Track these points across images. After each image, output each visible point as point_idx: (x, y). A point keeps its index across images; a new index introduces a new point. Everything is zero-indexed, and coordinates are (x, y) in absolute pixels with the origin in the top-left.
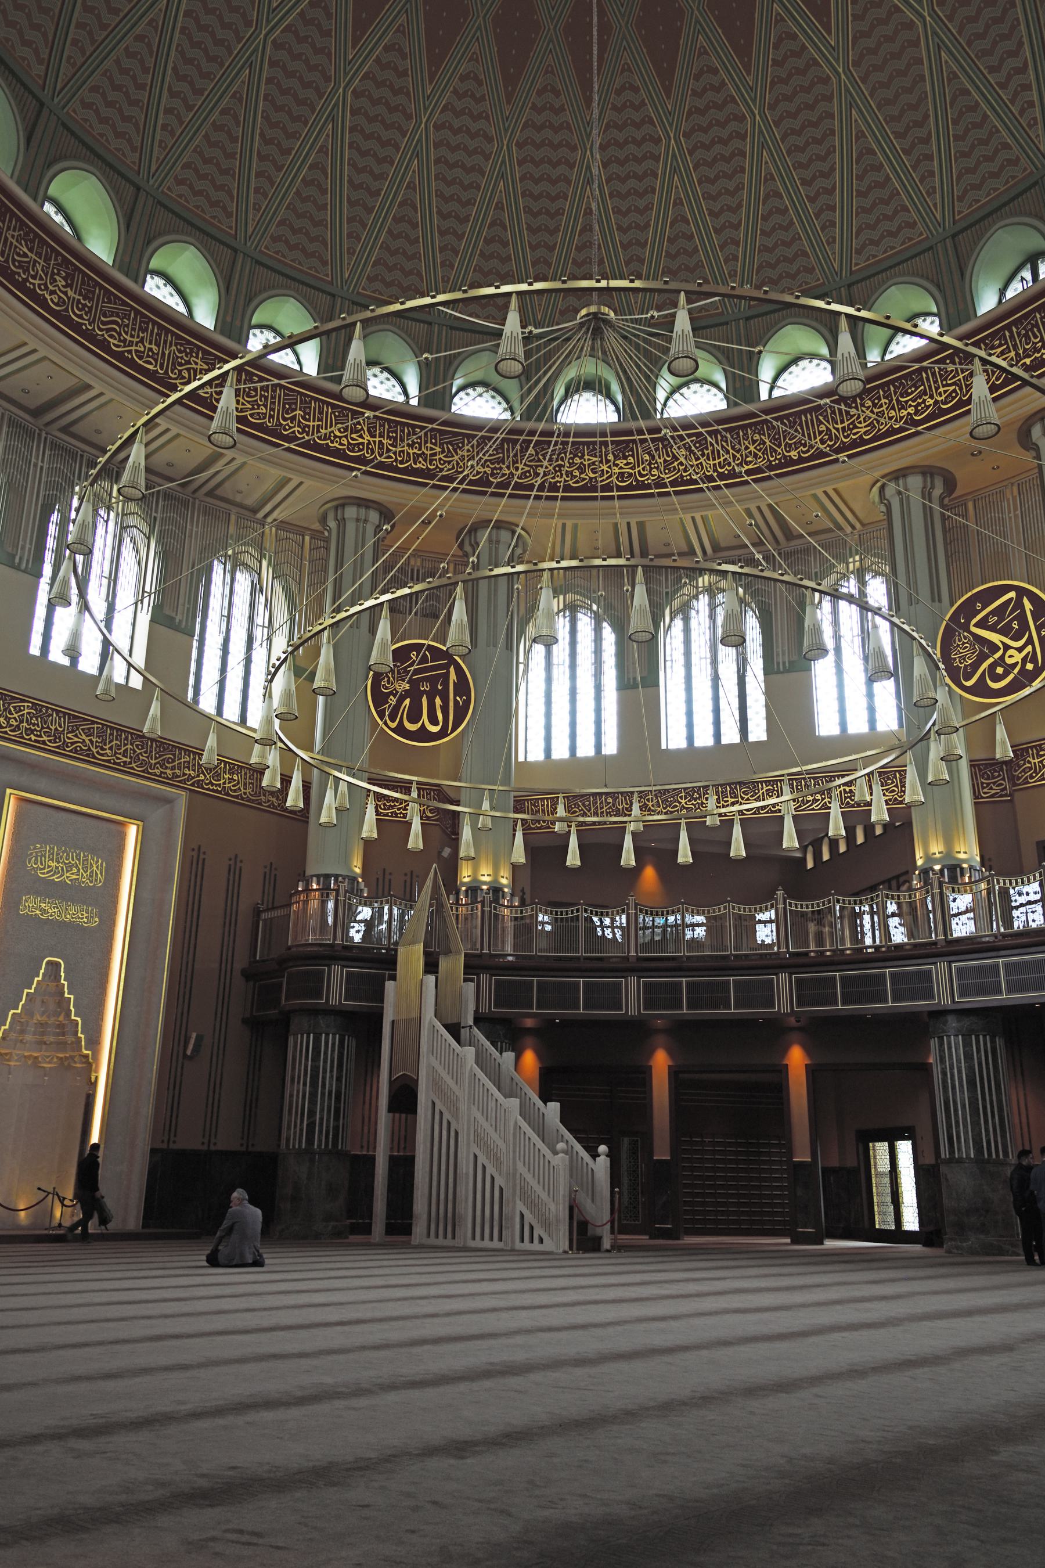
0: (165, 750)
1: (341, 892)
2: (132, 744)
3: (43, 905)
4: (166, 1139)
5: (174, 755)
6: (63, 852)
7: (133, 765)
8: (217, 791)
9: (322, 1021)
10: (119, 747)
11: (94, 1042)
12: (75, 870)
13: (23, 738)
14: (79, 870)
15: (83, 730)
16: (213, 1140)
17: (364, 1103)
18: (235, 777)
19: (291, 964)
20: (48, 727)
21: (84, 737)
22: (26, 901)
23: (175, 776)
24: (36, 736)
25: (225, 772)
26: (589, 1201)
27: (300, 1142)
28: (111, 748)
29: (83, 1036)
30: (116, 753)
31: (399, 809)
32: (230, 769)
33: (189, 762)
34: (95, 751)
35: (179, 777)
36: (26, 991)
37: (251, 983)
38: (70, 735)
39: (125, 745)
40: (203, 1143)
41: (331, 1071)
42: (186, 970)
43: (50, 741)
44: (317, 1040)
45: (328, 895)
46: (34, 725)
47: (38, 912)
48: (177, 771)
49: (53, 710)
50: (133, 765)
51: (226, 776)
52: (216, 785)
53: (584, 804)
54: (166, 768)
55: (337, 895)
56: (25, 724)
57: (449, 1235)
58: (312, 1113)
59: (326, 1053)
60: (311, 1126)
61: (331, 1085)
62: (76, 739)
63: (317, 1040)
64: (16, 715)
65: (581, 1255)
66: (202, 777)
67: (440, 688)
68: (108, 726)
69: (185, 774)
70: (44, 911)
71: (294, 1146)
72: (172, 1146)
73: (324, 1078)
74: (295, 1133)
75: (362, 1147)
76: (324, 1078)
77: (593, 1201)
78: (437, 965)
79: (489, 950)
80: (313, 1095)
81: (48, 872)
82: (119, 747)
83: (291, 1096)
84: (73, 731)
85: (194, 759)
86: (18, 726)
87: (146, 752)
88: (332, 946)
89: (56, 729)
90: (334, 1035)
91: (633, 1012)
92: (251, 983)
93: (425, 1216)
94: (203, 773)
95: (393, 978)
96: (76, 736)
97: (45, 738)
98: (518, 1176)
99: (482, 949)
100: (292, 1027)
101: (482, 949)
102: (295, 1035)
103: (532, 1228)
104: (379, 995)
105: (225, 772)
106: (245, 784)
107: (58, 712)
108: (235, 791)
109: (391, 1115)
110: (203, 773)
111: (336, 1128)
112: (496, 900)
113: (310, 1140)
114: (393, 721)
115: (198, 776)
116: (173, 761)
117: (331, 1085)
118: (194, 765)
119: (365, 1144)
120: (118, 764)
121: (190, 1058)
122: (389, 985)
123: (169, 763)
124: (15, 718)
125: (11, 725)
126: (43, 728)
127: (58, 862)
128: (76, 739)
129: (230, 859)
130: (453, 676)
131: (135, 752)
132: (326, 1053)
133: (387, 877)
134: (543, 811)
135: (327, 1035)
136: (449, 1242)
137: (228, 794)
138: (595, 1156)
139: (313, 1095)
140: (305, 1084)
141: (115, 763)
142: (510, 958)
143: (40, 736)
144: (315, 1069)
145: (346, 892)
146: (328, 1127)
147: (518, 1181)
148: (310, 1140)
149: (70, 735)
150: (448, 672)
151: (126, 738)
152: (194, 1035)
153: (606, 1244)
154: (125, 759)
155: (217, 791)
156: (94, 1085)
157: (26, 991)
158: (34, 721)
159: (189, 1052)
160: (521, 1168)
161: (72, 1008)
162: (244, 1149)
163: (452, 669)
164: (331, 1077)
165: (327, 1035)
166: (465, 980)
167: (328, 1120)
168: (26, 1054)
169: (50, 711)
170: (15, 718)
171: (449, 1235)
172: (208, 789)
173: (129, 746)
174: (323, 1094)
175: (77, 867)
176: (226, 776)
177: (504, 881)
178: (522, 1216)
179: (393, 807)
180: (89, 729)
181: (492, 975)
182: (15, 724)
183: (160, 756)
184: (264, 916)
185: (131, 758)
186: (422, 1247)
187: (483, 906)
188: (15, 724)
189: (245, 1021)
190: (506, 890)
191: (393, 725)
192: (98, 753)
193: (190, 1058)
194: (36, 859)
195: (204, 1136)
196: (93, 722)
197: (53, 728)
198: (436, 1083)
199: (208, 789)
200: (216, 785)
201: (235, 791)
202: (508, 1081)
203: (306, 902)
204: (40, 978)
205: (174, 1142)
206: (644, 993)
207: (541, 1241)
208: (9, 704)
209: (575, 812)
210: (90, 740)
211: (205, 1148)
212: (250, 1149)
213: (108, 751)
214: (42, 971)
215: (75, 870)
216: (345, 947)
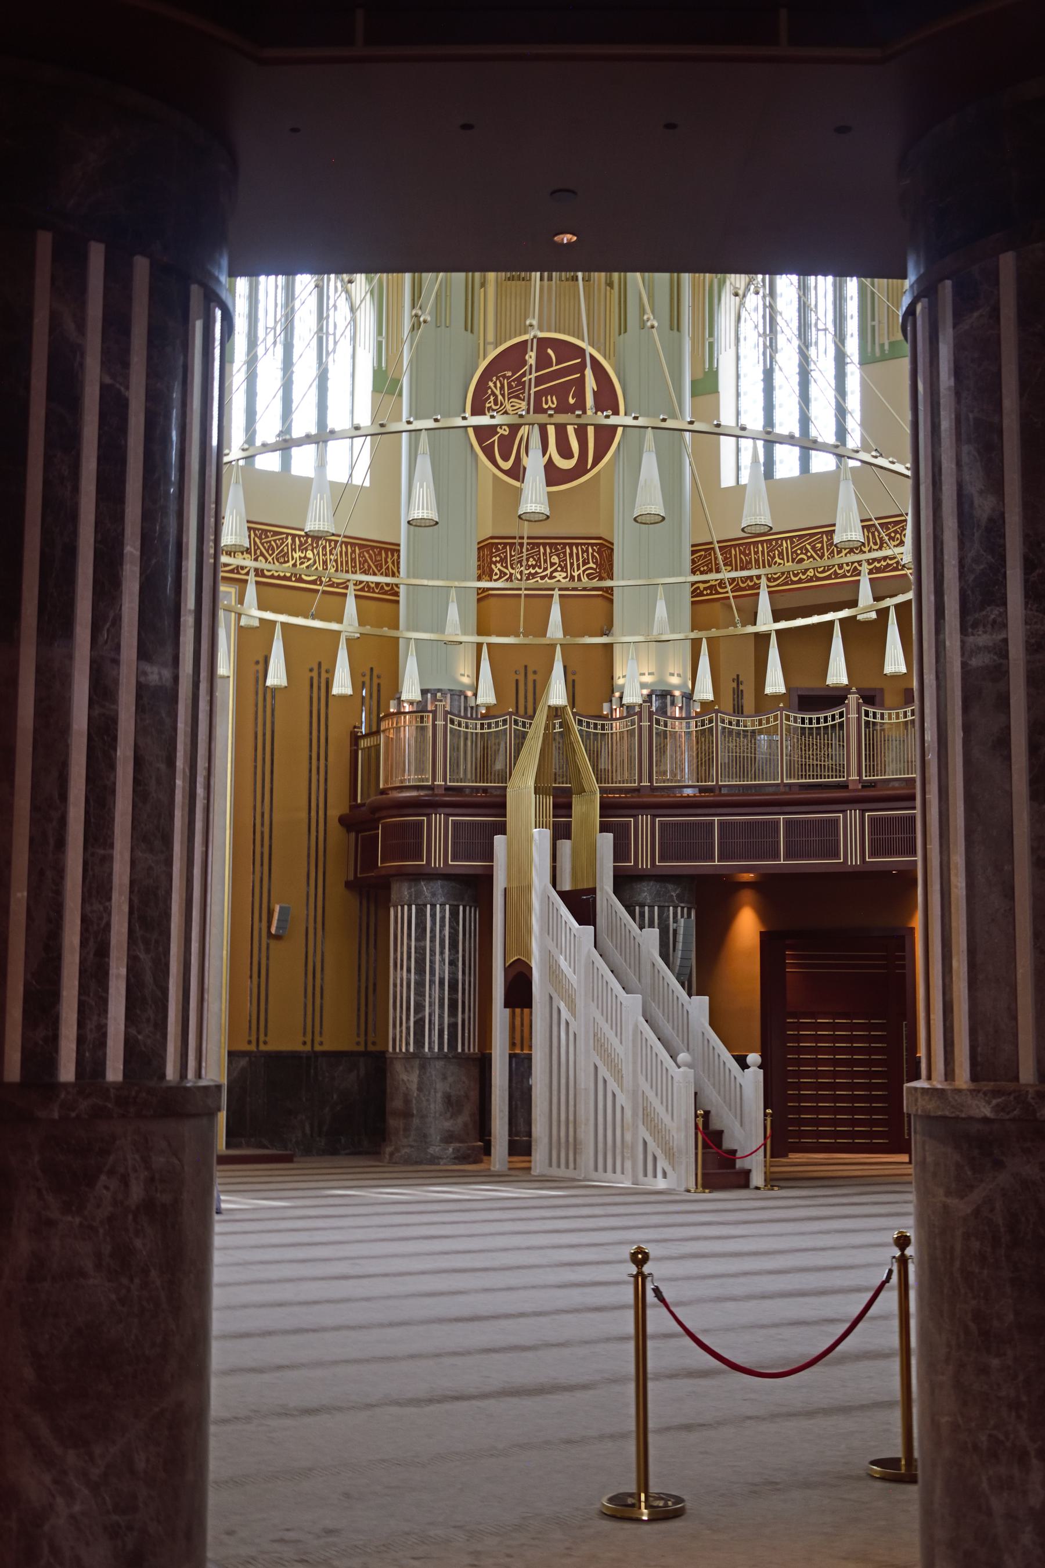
1: (440, 714)
4: (254, 1038)
9: (425, 888)
16: (317, 1039)
18: (310, 554)
19: (384, 813)
25: (293, 550)
26: (738, 1124)
27: (408, 1044)
31: (542, 578)
32: (301, 544)
37: (353, 835)
40: (304, 1043)
41: (442, 953)
42: (262, 825)
44: (421, 913)
45: (422, 717)
51: (297, 555)
53: (814, 548)
55: (434, 719)
57: (571, 1165)
58: (419, 1007)
59: (433, 931)
60: (419, 1023)
61: (442, 970)
63: (421, 913)
65: (708, 1195)
67: (572, 401)
71: (401, 1049)
72: (263, 1047)
73: (432, 962)
74: (401, 1032)
76: (432, 962)
77: (741, 1126)
78: (569, 806)
79: (651, 780)
80: (420, 984)
83: (395, 985)
88: (431, 788)
90: (442, 905)
91: (854, 860)
92: (353, 835)
93: (546, 1140)
95: (502, 829)
98: (640, 1093)
99: (640, 781)
100: (394, 897)
101: (640, 781)
102: (396, 907)
103: (655, 1158)
104: (488, 854)
105: (293, 550)
106: (325, 563)
109: (508, 1010)
110: (262, 554)
111: (453, 1026)
112: (663, 711)
113: (419, 1042)
114: (506, 458)
117: (442, 970)
119: (518, 1041)
121: (278, 937)
122: (499, 840)
129: (311, 670)
130: (591, 383)
132: (433, 931)
133: (531, 677)
134: (757, 561)
135: (433, 906)
136: (570, 1173)
137: (300, 580)
138: (744, 1065)
139: (420, 984)
140: (409, 971)
142: (689, 792)
144: (421, 951)
145: (446, 713)
146: (441, 1024)
147: (640, 1100)
148: (419, 1042)
150: (583, 376)
152: (277, 908)
153: (757, 1179)
159: (273, 931)
160: (644, 1086)
162: (362, 1048)
163: (588, 373)
164: (443, 960)
165: (433, 906)
166: (604, 828)
167: (441, 1017)
171: (571, 1165)
174: (432, 982)
176: (297, 555)
177: (675, 680)
178: (645, 1143)
181: (654, 816)
184: (364, 743)
186: (545, 1181)
187: (640, 720)
189: (348, 885)
190: (677, 693)
191: (507, 465)
193: (278, 937)
195: (304, 1034)
198: (553, 972)
202: (649, 967)
203: (398, 729)
205: (265, 1043)
206: (871, 833)
207: (665, 1175)
209: (802, 560)
211: (308, 1048)
212: (371, 1048)
216: (448, 789)
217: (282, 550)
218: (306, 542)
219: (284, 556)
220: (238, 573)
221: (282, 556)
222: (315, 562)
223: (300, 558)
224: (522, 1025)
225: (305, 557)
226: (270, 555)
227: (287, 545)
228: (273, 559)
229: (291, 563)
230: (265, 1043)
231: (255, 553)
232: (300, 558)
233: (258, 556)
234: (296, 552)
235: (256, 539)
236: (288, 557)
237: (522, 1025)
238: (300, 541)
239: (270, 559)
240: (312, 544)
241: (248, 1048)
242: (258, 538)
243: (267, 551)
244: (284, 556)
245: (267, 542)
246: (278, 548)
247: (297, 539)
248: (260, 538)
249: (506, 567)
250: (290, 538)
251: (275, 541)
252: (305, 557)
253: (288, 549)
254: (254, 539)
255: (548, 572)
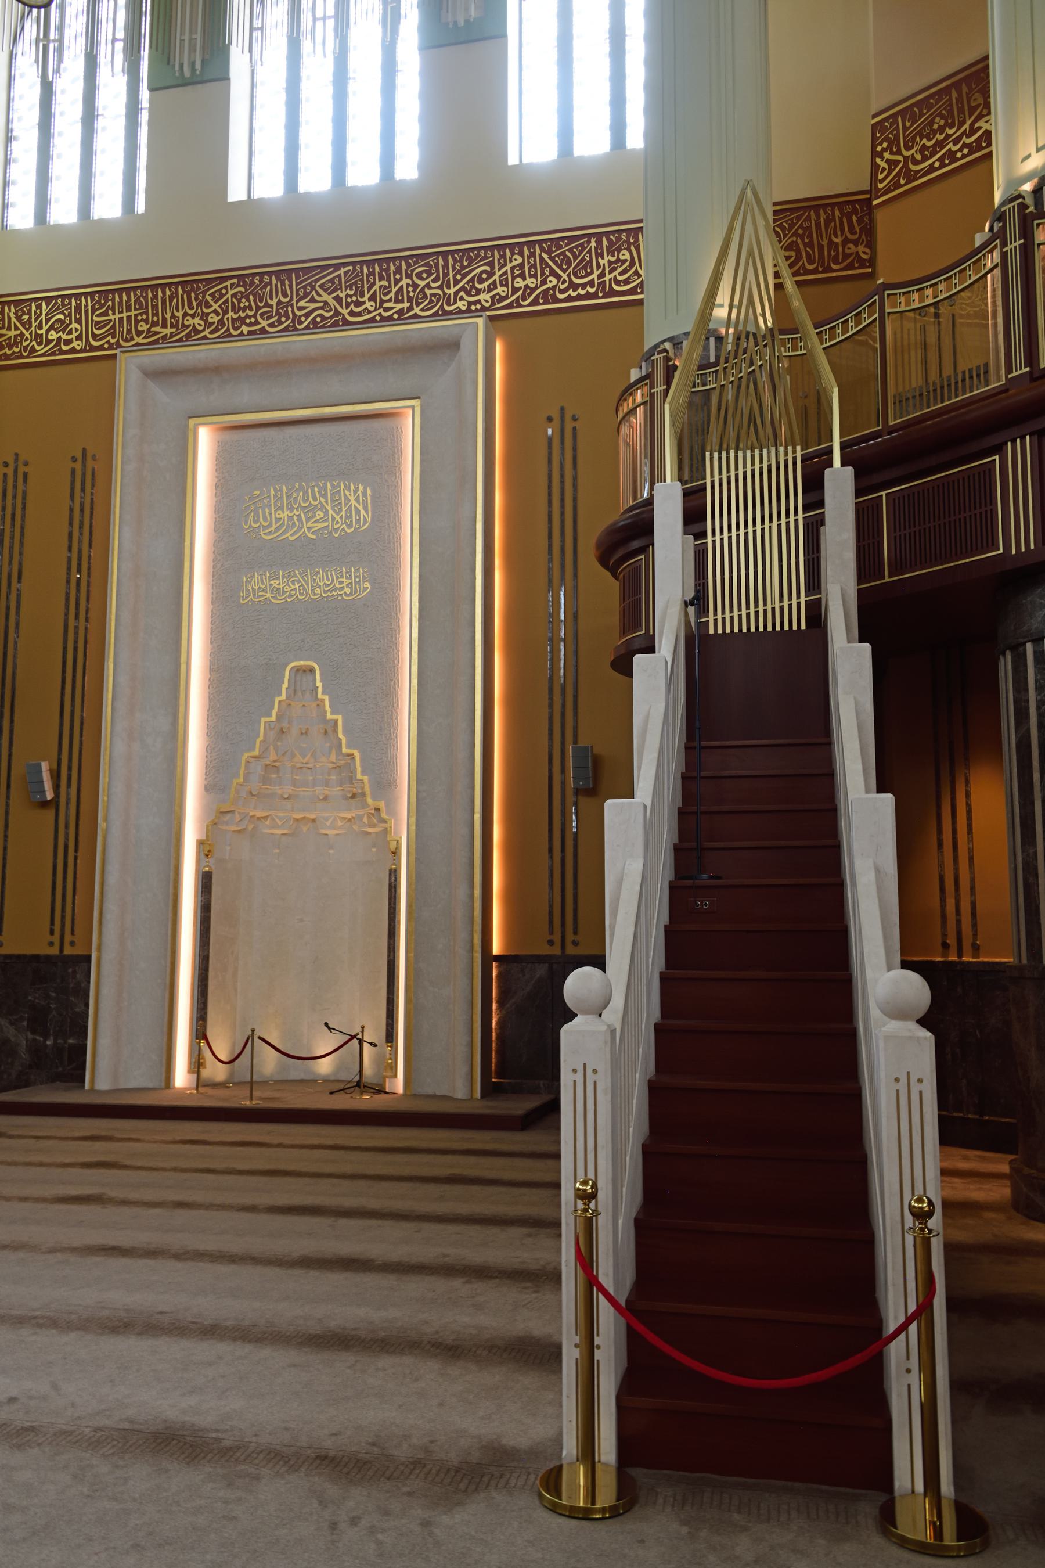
0: (471, 261)
2: (409, 276)
3: (275, 583)
4: (557, 938)
5: (491, 264)
6: (297, 491)
7: (417, 310)
8: (588, 296)
10: (386, 290)
11: (385, 785)
12: (320, 514)
13: (231, 335)
14: (326, 512)
15: (322, 286)
17: (940, 844)
20: (267, 305)
21: (326, 297)
22: (248, 582)
23: (497, 299)
24: (251, 324)
28: (372, 298)
29: (365, 778)
30: (382, 302)
33: (521, 266)
34: (345, 311)
35: (506, 297)
36: (263, 720)
38: (302, 304)
39: (397, 282)
43: (271, 325)
46: (244, 309)
47: (268, 595)
48: (501, 290)
49: (269, 274)
50: (417, 310)
52: (584, 286)
54: (479, 292)
56: (231, 314)
62: (313, 306)
64: (216, 306)
66: (552, 281)
68: (362, 263)
69: (515, 290)
70: (276, 591)
75: (945, 946)
81: (277, 530)
82: (386, 290)
84: (306, 295)
85: (532, 255)
86: (221, 322)
87: (435, 281)
89: (279, 303)
94: (553, 273)
96: (313, 300)
97: (264, 323)
107: (277, 274)
108: (627, 282)
110: (553, 273)
115: (544, 282)
116: (491, 274)
118: (534, 266)
119: (952, 941)
120: (390, 318)
123: (481, 281)
124: (215, 312)
125: (212, 324)
126: (258, 308)
127: (291, 509)
128: (313, 306)
131: (415, 286)
137: (613, 293)
141: (384, 319)
143: (257, 323)
149: (302, 304)
151: (398, 270)
154: (399, 306)
155: (588, 296)
156: (396, 853)
157: (263, 720)
158: (244, 303)
161: (341, 736)
168: (298, 816)
169: (266, 279)
170: (215, 312)
172: (570, 299)
173: (405, 281)
175: (323, 508)
179: (941, 144)
180: (332, 281)
182: (216, 319)
183: (464, 276)
185: (410, 299)
188: (216, 319)
192: (352, 314)
194: (257, 515)
196: (338, 267)
197: (274, 302)
199: (570, 299)
200: (584, 286)
201: (627, 282)
204: (284, 697)
208: (204, 293)
210: (338, 299)
213: (369, 305)
214: (285, 685)
215: (320, 514)
217: (583, 259)
218: (619, 239)
219: (585, 268)
220: (520, 306)
221: (581, 268)
222: (632, 264)
223: (610, 263)
224: (958, 912)
225: (618, 260)
226: (564, 271)
227: (590, 252)
228: (569, 276)
229: (596, 273)
230: (575, 943)
231: (543, 273)
232: (610, 263)
233: (548, 276)
234: (603, 258)
235: (545, 256)
236: (592, 267)
237: (958, 912)
238: (609, 240)
239: (564, 276)
240: (628, 241)
241: (545, 950)
242: (546, 252)
243: (560, 267)
244: (585, 268)
245: (558, 256)
246: (576, 257)
247: (604, 239)
248: (549, 252)
249: (899, 153)
250: (593, 240)
251: (570, 250)
252: (618, 260)
253: (591, 258)
254: (540, 255)
255: (966, 126)
